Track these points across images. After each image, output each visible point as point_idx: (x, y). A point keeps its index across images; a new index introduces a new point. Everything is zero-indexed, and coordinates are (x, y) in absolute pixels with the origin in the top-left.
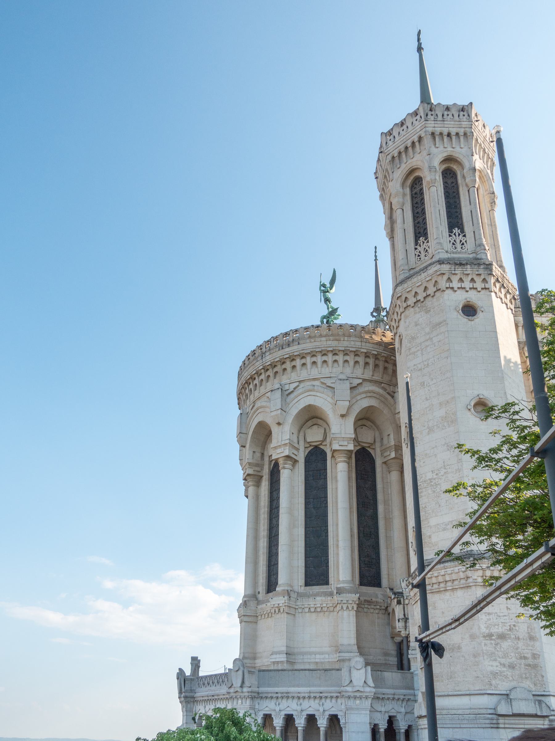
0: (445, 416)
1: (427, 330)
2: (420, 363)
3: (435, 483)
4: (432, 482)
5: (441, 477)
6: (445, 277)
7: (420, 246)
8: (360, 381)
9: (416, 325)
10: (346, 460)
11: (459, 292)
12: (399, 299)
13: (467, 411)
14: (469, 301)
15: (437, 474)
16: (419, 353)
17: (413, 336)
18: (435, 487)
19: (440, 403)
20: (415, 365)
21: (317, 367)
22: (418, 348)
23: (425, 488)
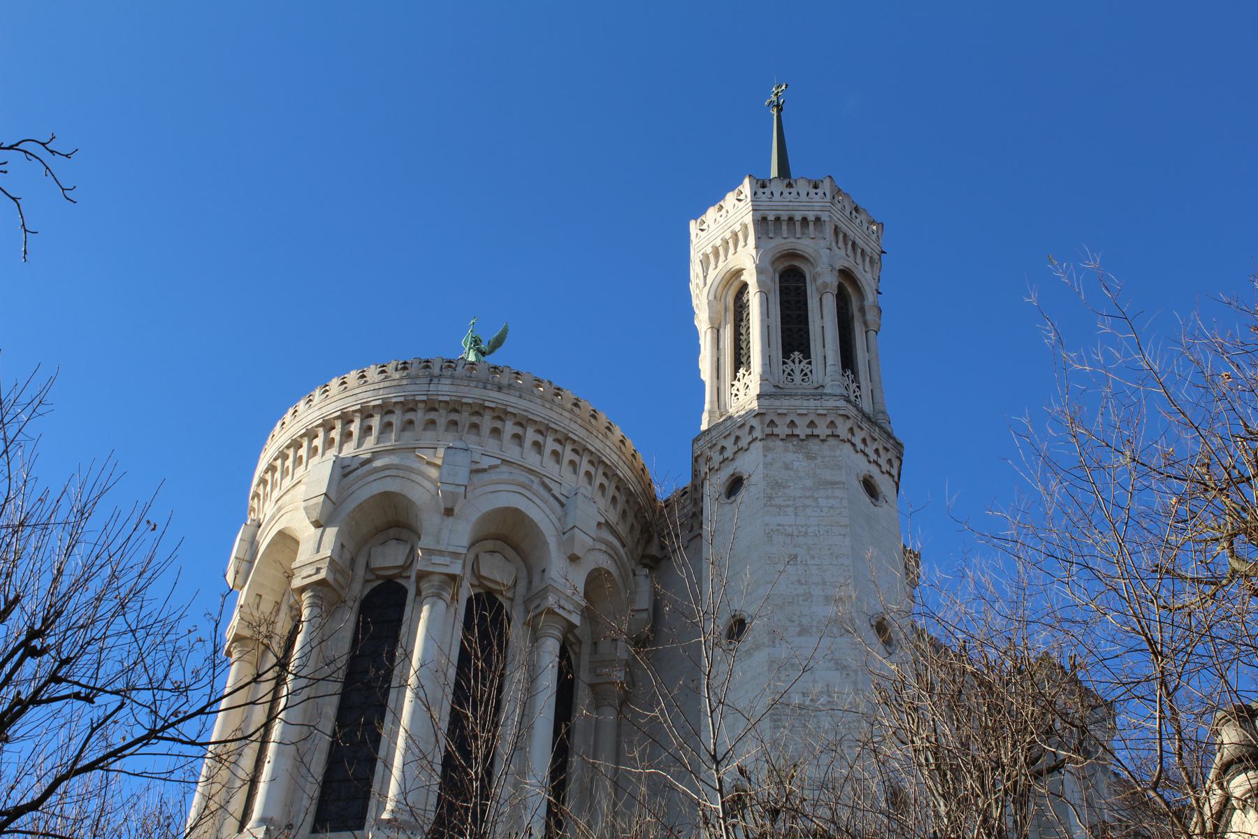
2: (790, 526)
6: (849, 424)
7: (793, 362)
10: (559, 634)
11: (860, 455)
12: (758, 418)
16: (790, 510)
20: (779, 525)
22: (791, 503)
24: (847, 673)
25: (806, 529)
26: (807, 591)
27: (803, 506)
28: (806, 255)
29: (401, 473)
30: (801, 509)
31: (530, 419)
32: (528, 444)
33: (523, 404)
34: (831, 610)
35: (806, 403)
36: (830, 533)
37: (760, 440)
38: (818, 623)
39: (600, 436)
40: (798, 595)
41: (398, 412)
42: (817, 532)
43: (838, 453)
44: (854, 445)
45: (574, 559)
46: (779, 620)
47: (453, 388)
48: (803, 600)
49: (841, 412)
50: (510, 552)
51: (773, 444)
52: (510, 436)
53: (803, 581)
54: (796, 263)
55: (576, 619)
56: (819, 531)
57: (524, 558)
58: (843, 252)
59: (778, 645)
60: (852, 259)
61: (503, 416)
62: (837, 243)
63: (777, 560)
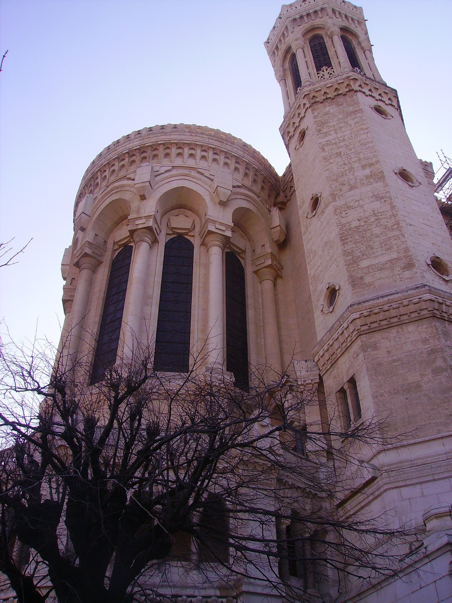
2: (334, 139)
11: (369, 98)
12: (306, 98)
20: (327, 141)
24: (384, 200)
28: (320, 26)
29: (119, 190)
31: (184, 143)
32: (186, 155)
34: (367, 172)
37: (309, 108)
39: (229, 144)
40: (345, 171)
41: (117, 164)
42: (350, 137)
43: (355, 97)
44: (364, 93)
46: (337, 186)
47: (141, 142)
49: (352, 78)
50: (188, 212)
53: (347, 163)
54: (317, 32)
55: (229, 234)
56: (351, 136)
57: (197, 214)
58: (340, 20)
59: (337, 199)
60: (346, 22)
61: (170, 146)
62: (336, 16)
63: (329, 157)
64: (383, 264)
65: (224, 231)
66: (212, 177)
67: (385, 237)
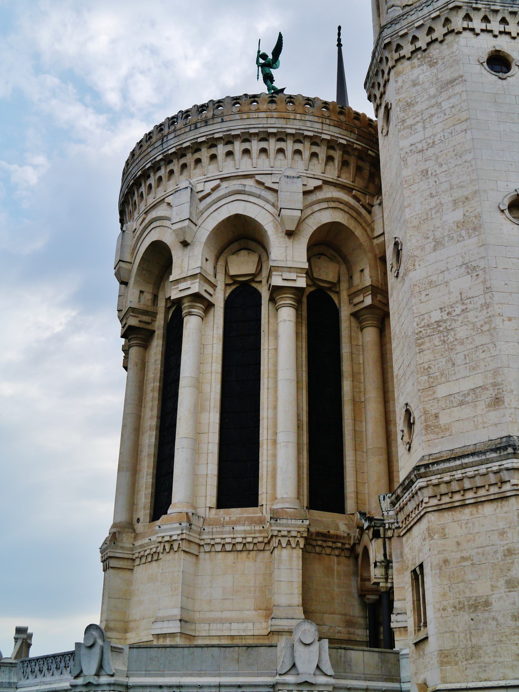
0: (462, 221)
1: (432, 91)
2: (420, 142)
3: (446, 327)
4: (440, 326)
5: (455, 318)
6: (462, 13)
8: (320, 183)
9: (414, 85)
10: (293, 303)
11: (483, 35)
12: (387, 48)
13: (499, 213)
14: (499, 51)
15: (448, 313)
16: (419, 127)
17: (409, 101)
18: (446, 334)
19: (455, 201)
20: (412, 145)
21: (251, 158)
22: (418, 119)
23: (429, 336)
24: (476, 274)
25: (434, 139)
26: (438, 201)
27: (429, 117)
30: (428, 120)
32: (238, 153)
33: (225, 126)
35: (420, 14)
36: (453, 134)
38: (449, 231)
39: (298, 117)
43: (456, 46)
45: (290, 234)
48: (435, 213)
51: (402, 66)
52: (224, 156)
56: (444, 136)
59: (417, 267)
64: (465, 394)
65: (295, 280)
66: (275, 186)
67: (472, 346)
